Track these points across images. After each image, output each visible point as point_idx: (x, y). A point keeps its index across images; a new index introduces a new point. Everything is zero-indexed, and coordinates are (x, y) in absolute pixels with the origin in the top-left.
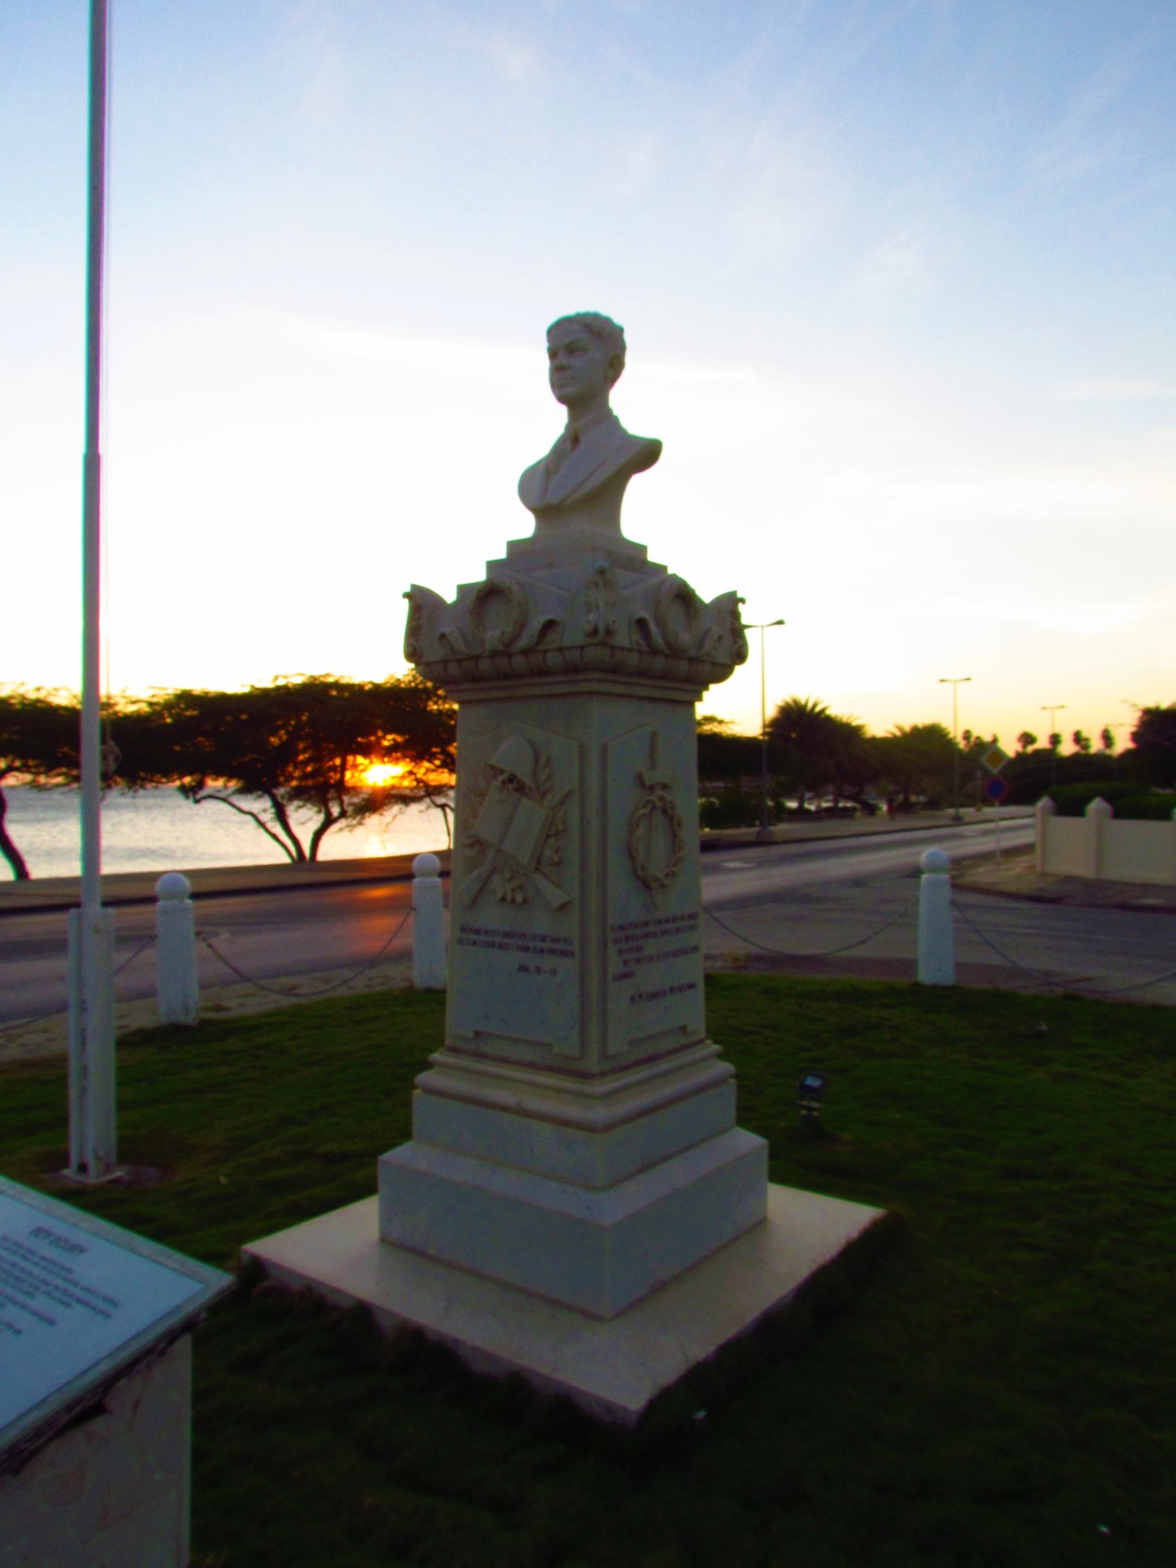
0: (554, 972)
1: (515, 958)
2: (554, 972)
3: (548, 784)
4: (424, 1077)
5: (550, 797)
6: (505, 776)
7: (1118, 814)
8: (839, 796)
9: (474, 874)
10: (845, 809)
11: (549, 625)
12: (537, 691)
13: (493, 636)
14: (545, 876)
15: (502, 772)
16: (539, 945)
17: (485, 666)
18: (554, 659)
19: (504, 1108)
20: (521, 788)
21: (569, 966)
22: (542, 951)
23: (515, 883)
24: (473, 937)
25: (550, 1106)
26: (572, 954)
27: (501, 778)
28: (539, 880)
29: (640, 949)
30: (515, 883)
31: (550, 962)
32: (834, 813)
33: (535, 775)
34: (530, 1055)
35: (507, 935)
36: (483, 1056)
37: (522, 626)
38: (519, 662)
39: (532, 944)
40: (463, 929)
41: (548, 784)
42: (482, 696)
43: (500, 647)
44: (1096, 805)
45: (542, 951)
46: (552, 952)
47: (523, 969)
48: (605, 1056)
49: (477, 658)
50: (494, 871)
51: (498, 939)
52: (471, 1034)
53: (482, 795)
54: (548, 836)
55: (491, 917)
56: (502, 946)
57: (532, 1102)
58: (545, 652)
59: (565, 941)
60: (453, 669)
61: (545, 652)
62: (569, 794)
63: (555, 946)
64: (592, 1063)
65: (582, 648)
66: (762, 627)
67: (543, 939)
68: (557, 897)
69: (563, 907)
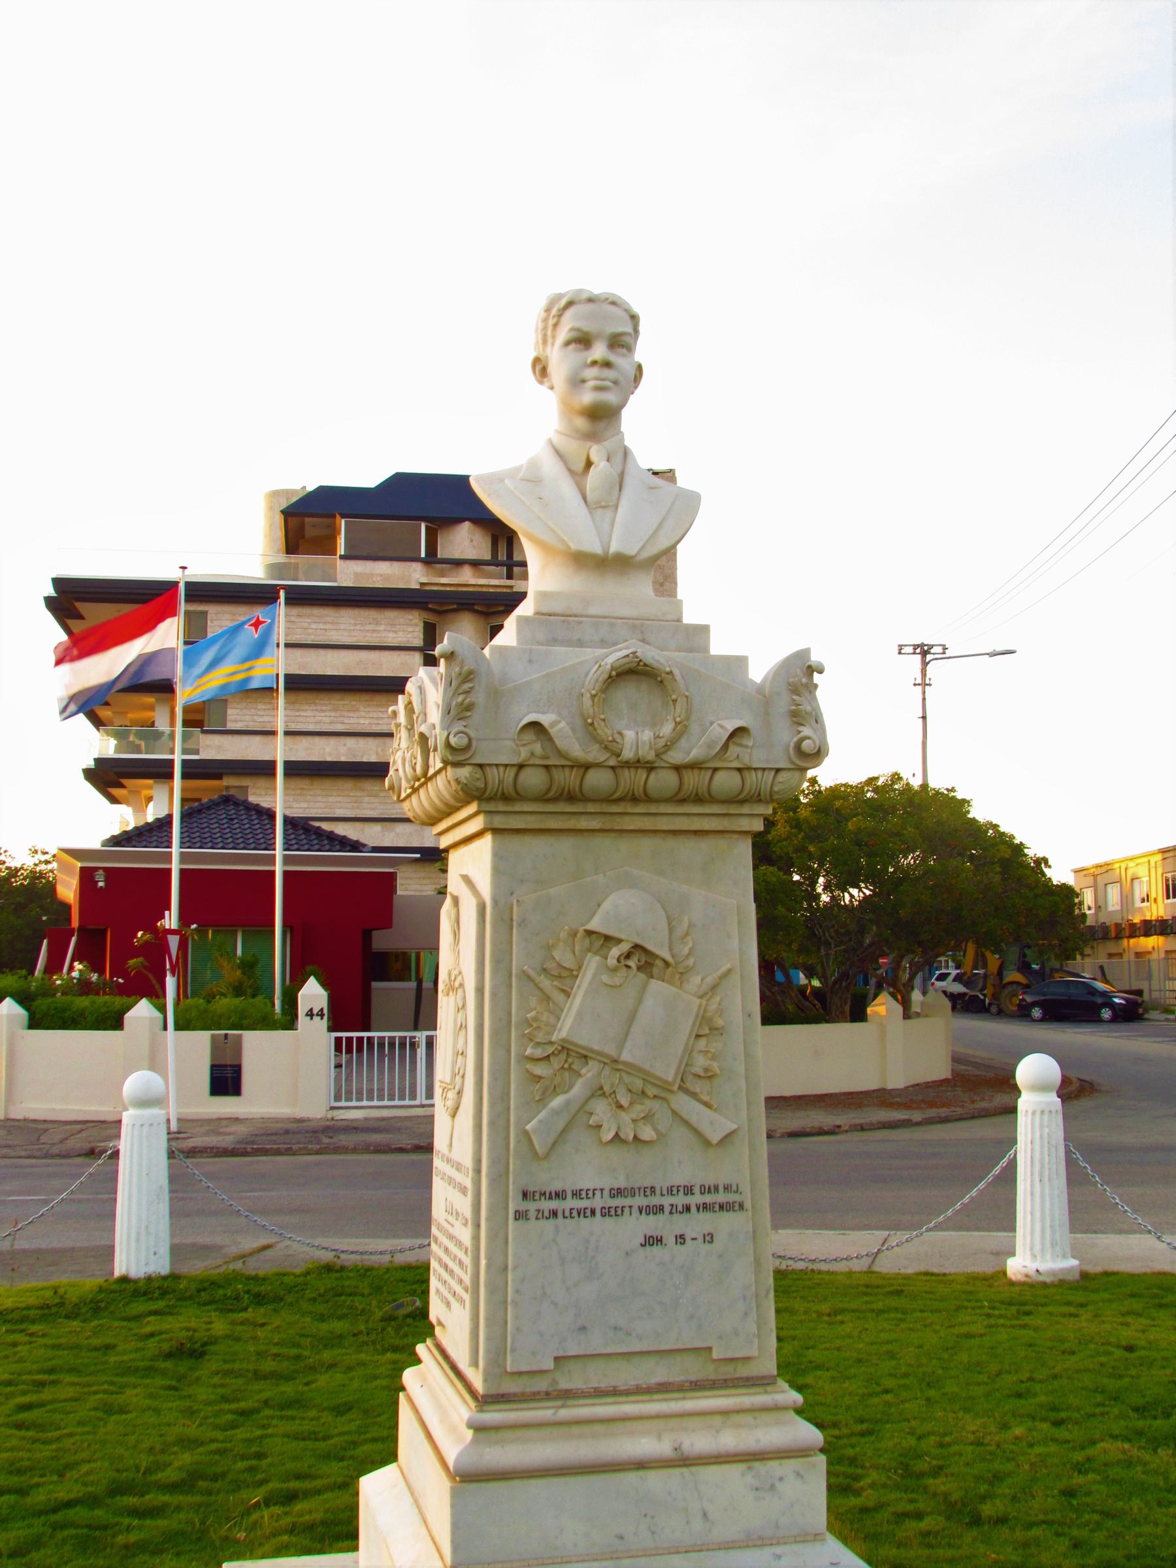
0: (709, 1238)
1: (636, 1226)
3: (691, 961)
5: (697, 980)
6: (625, 947)
7: (35, 1023)
9: (557, 1102)
11: (740, 731)
12: (663, 824)
14: (694, 1095)
15: (609, 940)
16: (680, 1200)
17: (598, 780)
18: (726, 782)
19: (641, 1465)
22: (688, 1209)
24: (547, 1205)
25: (729, 1440)
26: (741, 1206)
27: (615, 952)
30: (639, 1110)
33: (671, 950)
34: (660, 1373)
35: (617, 1192)
36: (567, 1395)
37: (681, 729)
38: (663, 781)
39: (667, 1201)
40: (525, 1195)
42: (552, 823)
43: (651, 756)
45: (688, 1209)
46: (705, 1207)
47: (653, 1241)
49: (587, 767)
50: (599, 1092)
51: (598, 1202)
52: (549, 1364)
53: (567, 977)
54: (698, 1036)
56: (606, 1212)
57: (699, 1442)
58: (715, 770)
59: (727, 1188)
61: (715, 770)
62: (729, 971)
63: (708, 1198)
65: (778, 770)
67: (689, 1190)
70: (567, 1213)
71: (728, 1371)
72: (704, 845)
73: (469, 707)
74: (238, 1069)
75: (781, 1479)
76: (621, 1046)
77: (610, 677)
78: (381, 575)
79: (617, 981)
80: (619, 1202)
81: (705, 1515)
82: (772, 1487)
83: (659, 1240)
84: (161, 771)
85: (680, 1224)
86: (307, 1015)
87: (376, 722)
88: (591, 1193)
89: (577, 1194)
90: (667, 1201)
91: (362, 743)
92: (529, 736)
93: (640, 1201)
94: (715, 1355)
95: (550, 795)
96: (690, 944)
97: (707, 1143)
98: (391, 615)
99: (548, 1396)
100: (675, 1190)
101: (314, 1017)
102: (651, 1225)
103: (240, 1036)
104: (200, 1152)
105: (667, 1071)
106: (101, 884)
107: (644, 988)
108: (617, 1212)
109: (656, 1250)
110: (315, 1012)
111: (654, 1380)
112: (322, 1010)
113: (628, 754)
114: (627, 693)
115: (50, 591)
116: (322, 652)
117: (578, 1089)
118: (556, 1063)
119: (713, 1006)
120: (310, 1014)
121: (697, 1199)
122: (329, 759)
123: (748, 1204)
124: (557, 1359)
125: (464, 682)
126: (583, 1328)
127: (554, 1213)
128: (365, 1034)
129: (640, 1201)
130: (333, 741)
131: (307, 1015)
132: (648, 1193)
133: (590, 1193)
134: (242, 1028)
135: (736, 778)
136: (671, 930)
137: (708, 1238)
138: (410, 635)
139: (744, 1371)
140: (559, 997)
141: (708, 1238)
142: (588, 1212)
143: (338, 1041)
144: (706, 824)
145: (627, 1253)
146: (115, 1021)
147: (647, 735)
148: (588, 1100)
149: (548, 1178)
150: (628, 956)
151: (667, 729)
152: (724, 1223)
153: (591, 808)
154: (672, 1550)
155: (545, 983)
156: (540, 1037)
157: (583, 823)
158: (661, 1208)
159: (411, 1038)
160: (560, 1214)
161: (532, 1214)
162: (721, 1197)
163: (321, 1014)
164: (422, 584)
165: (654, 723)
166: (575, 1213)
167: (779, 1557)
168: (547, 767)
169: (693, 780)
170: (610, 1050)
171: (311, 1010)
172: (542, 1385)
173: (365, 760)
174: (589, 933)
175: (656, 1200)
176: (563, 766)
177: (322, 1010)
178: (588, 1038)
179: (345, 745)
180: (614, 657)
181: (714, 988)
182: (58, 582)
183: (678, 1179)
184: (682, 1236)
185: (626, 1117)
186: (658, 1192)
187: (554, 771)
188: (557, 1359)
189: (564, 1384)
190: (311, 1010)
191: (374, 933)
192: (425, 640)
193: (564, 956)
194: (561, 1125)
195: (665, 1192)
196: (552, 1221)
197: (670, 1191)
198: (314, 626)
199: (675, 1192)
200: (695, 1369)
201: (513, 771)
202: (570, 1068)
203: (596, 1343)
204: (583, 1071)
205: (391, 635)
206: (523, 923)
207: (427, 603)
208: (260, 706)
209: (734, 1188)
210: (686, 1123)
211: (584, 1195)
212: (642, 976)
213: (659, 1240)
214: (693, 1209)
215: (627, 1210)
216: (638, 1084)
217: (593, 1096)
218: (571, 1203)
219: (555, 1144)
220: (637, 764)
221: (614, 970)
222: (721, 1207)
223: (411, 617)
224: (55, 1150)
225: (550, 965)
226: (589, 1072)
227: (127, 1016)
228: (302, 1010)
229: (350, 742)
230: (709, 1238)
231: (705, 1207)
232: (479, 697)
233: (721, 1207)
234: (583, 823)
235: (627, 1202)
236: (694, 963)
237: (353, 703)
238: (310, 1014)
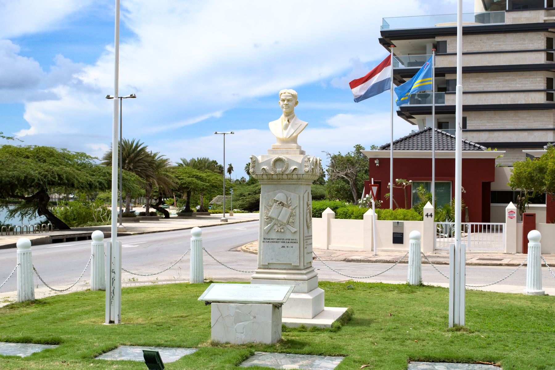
0: (292, 247)
1: (281, 244)
5: (291, 207)
6: (279, 202)
7: (337, 216)
8: (148, 206)
10: (153, 214)
11: (295, 169)
13: (279, 170)
15: (277, 201)
16: (288, 241)
17: (275, 177)
20: (283, 205)
21: (297, 245)
23: (281, 227)
27: (278, 203)
28: (288, 226)
30: (281, 227)
31: (290, 245)
32: (146, 216)
35: (278, 239)
36: (270, 269)
37: (287, 168)
38: (285, 177)
39: (286, 241)
44: (328, 211)
46: (292, 242)
48: (304, 266)
50: (275, 224)
51: (275, 241)
53: (271, 206)
55: (273, 235)
59: (295, 240)
62: (297, 206)
63: (292, 241)
64: (302, 267)
66: (121, 98)
67: (289, 240)
68: (294, 230)
69: (295, 232)
71: (295, 268)
72: (295, 186)
73: (255, 166)
74: (402, 234)
76: (278, 217)
78: (525, 18)
79: (278, 207)
80: (278, 241)
82: (299, 285)
83: (284, 247)
84: (427, 111)
85: (288, 245)
86: (426, 216)
87: (524, 85)
89: (272, 239)
90: (286, 241)
91: (518, 95)
92: (263, 170)
93: (281, 241)
94: (292, 265)
97: (292, 232)
98: (531, 35)
99: (267, 269)
101: (429, 216)
103: (403, 223)
104: (378, 261)
105: (285, 221)
106: (377, 165)
107: (283, 207)
109: (284, 248)
110: (429, 214)
111: (283, 268)
112: (431, 214)
113: (278, 173)
114: (278, 163)
115: (380, 37)
116: (498, 55)
117: (272, 224)
118: (269, 219)
119: (293, 211)
120: (427, 215)
121: (290, 241)
122: (502, 103)
123: (298, 242)
124: (268, 263)
125: (254, 162)
126: (272, 259)
128: (487, 224)
129: (281, 241)
130: (504, 95)
131: (426, 216)
133: (274, 239)
134: (404, 220)
138: (540, 45)
139: (297, 268)
143: (463, 225)
144: (294, 183)
146: (360, 217)
147: (280, 169)
148: (274, 225)
149: (267, 237)
150: (280, 203)
151: (284, 169)
152: (294, 245)
154: (422, 358)
156: (267, 216)
157: (275, 183)
158: (285, 242)
159: (465, 225)
162: (294, 241)
163: (431, 215)
164: (544, 20)
165: (283, 168)
169: (289, 177)
170: (276, 218)
171: (427, 214)
172: (267, 267)
173: (519, 103)
174: (274, 200)
175: (284, 241)
177: (431, 214)
178: (273, 216)
179: (510, 97)
180: (275, 157)
181: (294, 209)
182: (383, 33)
183: (287, 238)
185: (279, 228)
188: (268, 263)
189: (270, 267)
190: (427, 214)
191: (491, 183)
192: (547, 46)
193: (271, 203)
194: (269, 229)
198: (494, 44)
200: (290, 267)
201: (261, 175)
203: (274, 261)
205: (531, 45)
206: (265, 198)
207: (548, 29)
208: (471, 81)
210: (289, 229)
212: (282, 206)
213: (284, 247)
216: (281, 223)
218: (271, 240)
219: (268, 232)
220: (279, 174)
221: (278, 206)
223: (540, 36)
224: (334, 259)
225: (269, 204)
226: (274, 221)
227: (364, 215)
228: (425, 214)
229: (512, 95)
230: (292, 247)
231: (292, 242)
232: (256, 164)
234: (275, 183)
237: (514, 77)
238: (427, 215)
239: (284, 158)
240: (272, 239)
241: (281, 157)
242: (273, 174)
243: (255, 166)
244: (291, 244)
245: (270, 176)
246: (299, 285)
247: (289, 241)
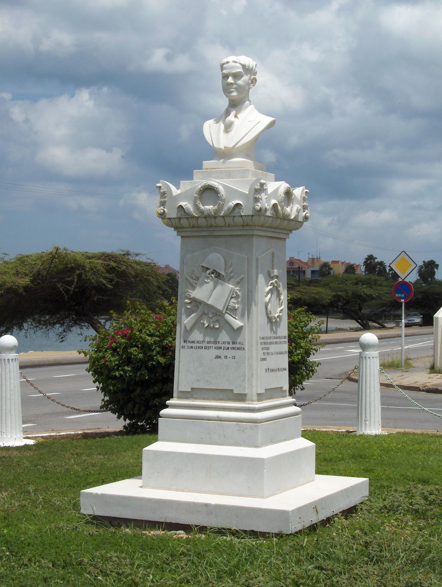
2: (234, 358)
3: (232, 275)
4: (164, 412)
11: (238, 205)
15: (208, 269)
16: (226, 346)
17: (202, 222)
22: (228, 348)
27: (208, 272)
29: (268, 349)
39: (222, 346)
41: (232, 275)
45: (228, 348)
46: (233, 348)
47: (218, 357)
52: (190, 390)
54: (232, 298)
56: (206, 348)
58: (234, 216)
60: (184, 222)
70: (195, 348)
73: (165, 202)
75: (246, 429)
76: (208, 299)
77: (201, 190)
81: (224, 436)
82: (244, 431)
83: (220, 357)
85: (226, 353)
88: (202, 342)
89: (198, 342)
90: (222, 346)
95: (208, 226)
96: (231, 270)
100: (225, 343)
102: (218, 352)
108: (208, 348)
118: (193, 304)
123: (246, 348)
124: (192, 389)
126: (198, 380)
127: (192, 347)
132: (217, 343)
135: (240, 219)
136: (226, 265)
137: (234, 357)
140: (195, 285)
141: (234, 357)
142: (201, 347)
145: (211, 360)
153: (204, 229)
155: (191, 280)
157: (204, 234)
158: (221, 348)
160: (193, 348)
161: (186, 347)
166: (197, 348)
167: (242, 450)
168: (187, 218)
174: (203, 266)
176: (191, 218)
184: (226, 356)
186: (220, 343)
187: (208, 219)
188: (192, 389)
195: (222, 343)
196: (191, 349)
197: (224, 343)
199: (225, 343)
202: (197, 306)
204: (200, 307)
209: (242, 343)
211: (200, 343)
213: (220, 357)
214: (230, 349)
215: (211, 348)
216: (214, 312)
217: (202, 314)
222: (238, 349)
225: (193, 276)
230: (234, 358)
233: (238, 349)
234: (204, 234)
235: (211, 345)
236: (233, 275)
239: (221, 189)
240: (198, 342)
241: (214, 183)
242: (198, 218)
243: (165, 202)
244: (232, 351)
245: (193, 222)
246: (244, 431)
247: (229, 346)
